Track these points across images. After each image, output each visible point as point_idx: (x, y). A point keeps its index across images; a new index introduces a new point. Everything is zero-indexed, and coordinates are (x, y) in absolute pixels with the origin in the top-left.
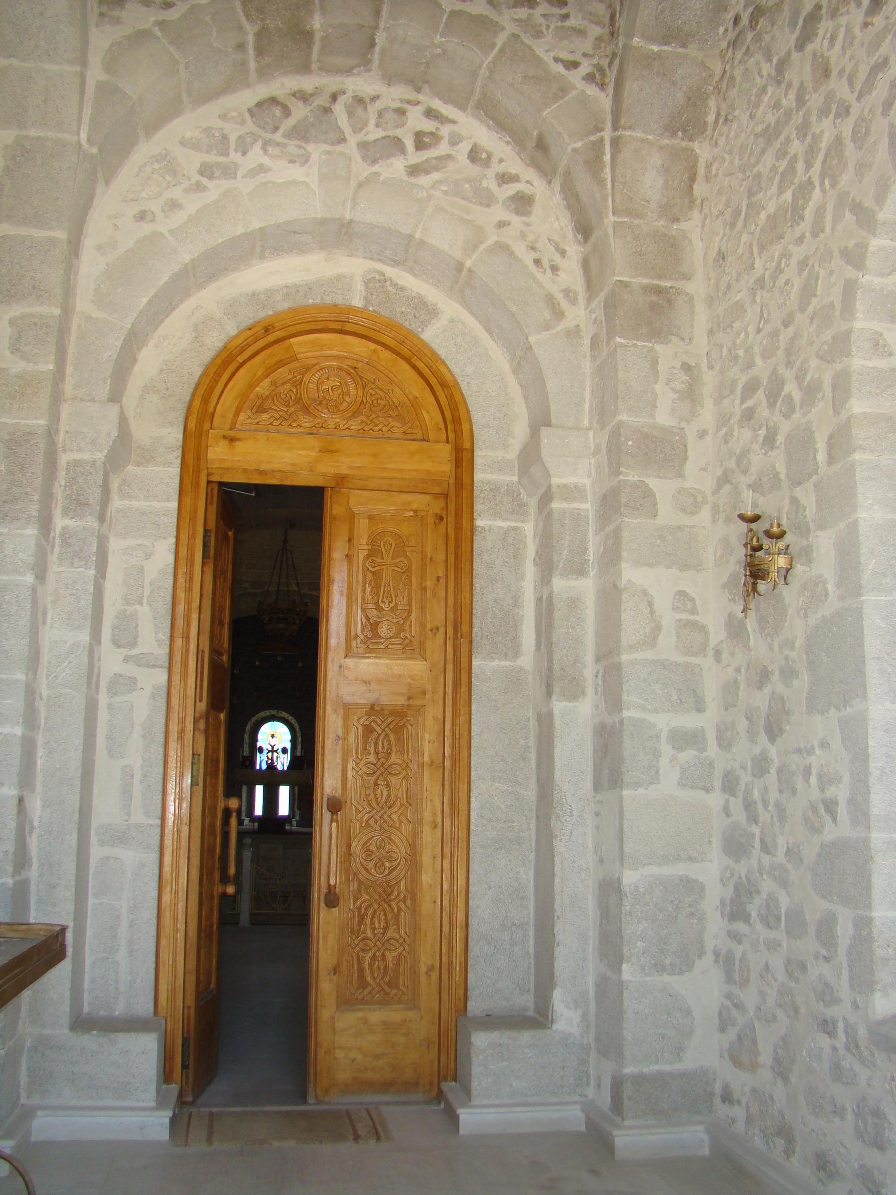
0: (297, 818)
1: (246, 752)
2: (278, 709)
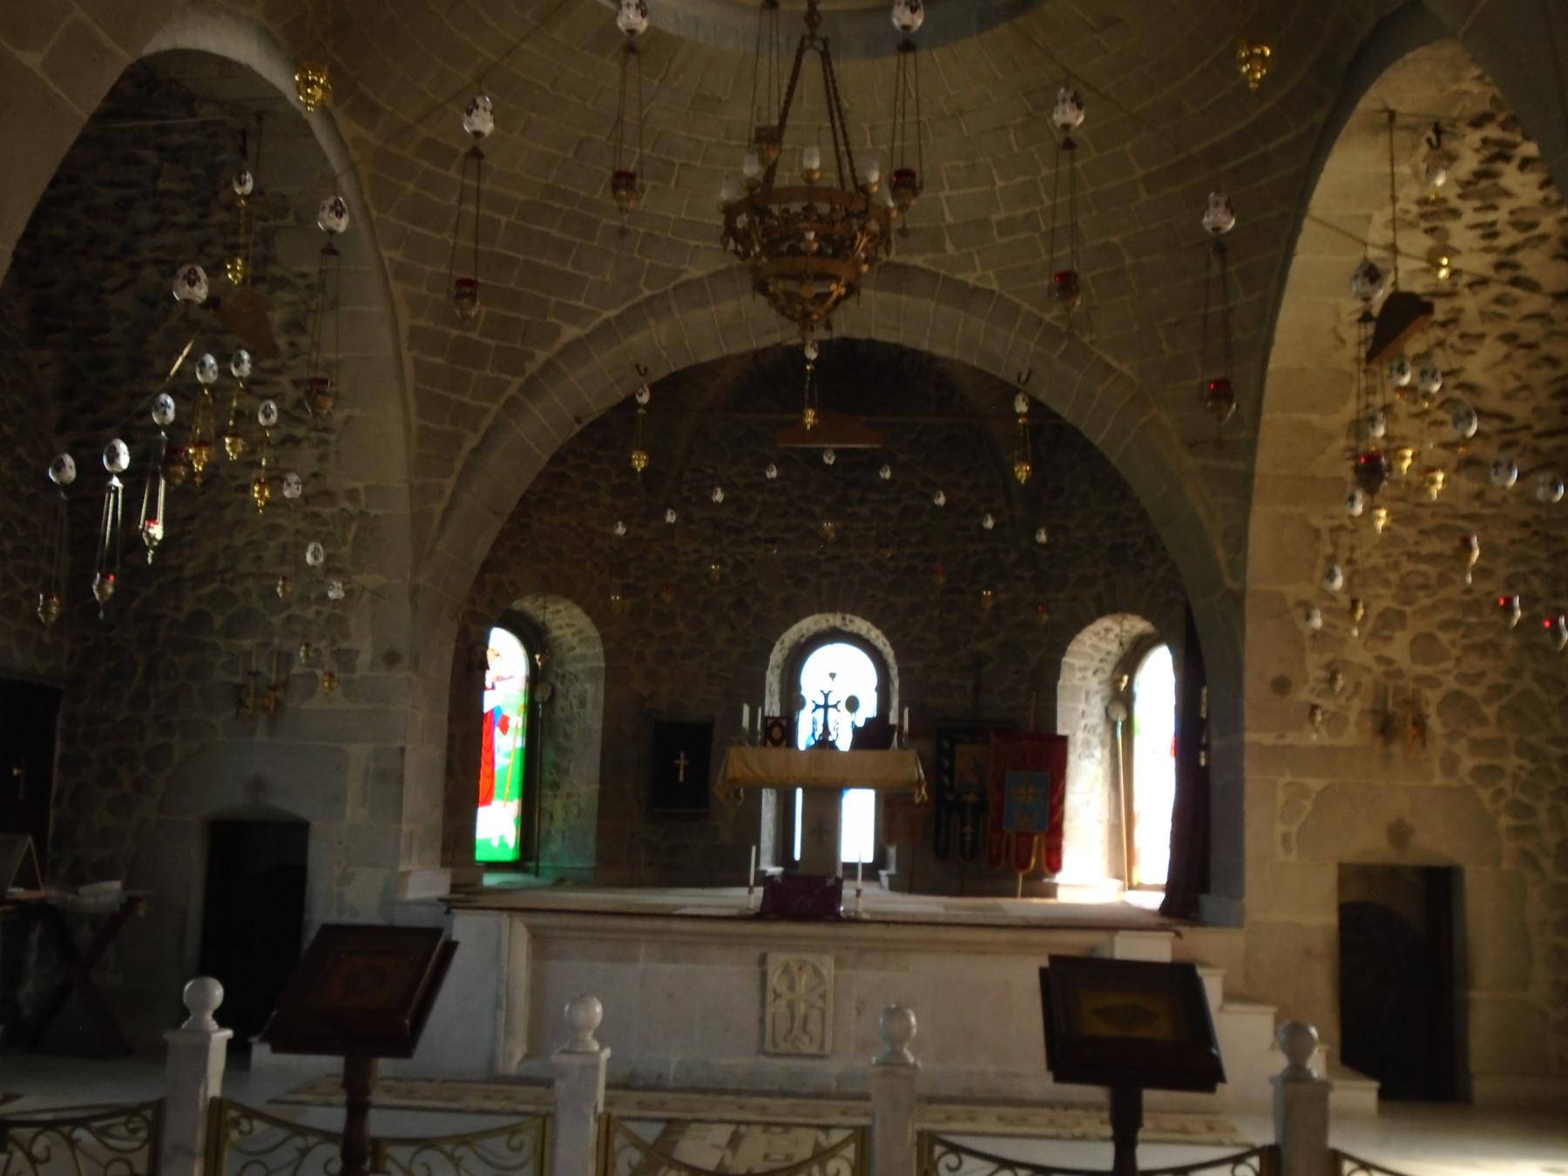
0: (892, 870)
1: (772, 707)
2: (844, 610)
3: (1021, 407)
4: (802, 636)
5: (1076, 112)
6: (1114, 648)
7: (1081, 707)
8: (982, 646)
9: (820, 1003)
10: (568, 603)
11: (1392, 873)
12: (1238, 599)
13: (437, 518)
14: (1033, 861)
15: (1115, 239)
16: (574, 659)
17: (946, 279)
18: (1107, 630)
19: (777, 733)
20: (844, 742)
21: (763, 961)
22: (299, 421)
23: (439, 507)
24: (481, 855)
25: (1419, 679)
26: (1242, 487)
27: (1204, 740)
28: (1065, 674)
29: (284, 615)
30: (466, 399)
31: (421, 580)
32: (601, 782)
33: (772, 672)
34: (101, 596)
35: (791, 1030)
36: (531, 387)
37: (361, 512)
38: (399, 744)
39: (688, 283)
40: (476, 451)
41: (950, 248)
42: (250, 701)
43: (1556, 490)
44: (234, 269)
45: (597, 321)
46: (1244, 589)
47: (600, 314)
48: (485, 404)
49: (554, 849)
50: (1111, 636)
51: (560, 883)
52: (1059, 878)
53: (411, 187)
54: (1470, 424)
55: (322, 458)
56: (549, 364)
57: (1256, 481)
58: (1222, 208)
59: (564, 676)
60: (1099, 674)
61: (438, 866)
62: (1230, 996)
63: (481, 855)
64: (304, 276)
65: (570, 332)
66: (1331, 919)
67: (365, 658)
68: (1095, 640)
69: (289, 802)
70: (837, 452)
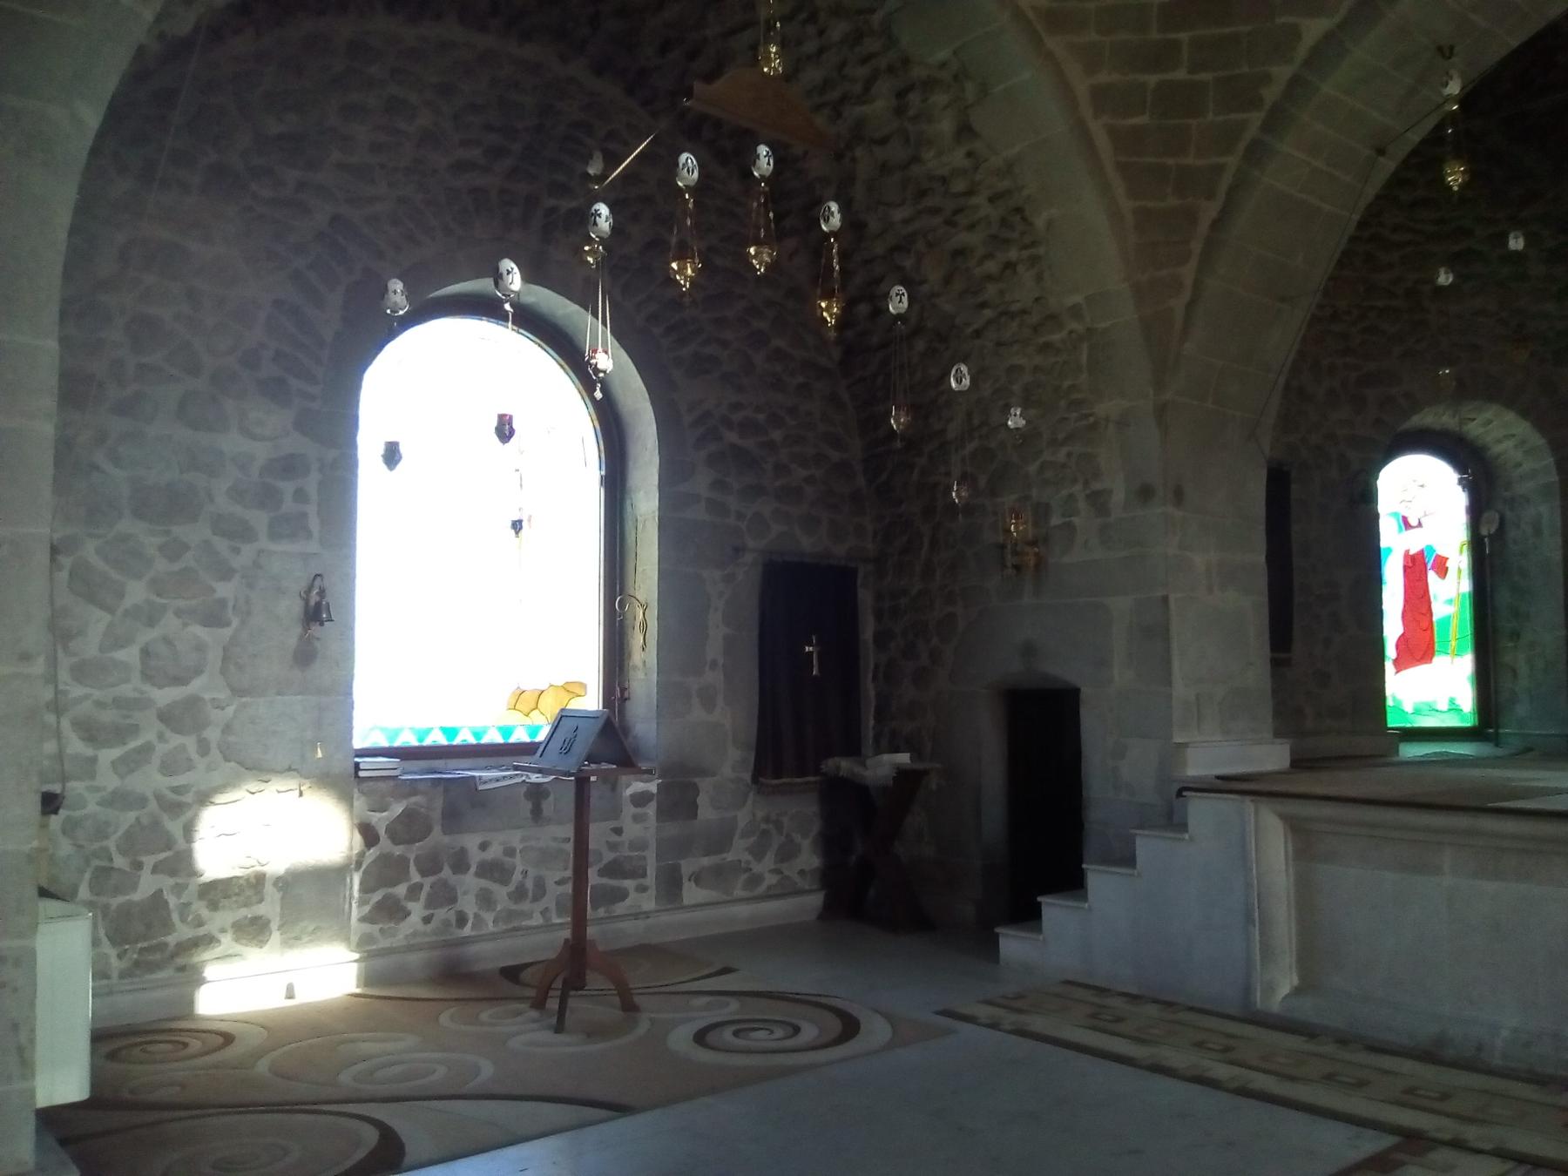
22: (1007, 241)
23: (1178, 304)
24: (1393, 721)
29: (1038, 463)
30: (1190, 160)
36: (1277, 121)
37: (1088, 329)
40: (1217, 224)
44: (768, 61)
48: (1221, 160)
49: (1521, 715)
55: (1039, 278)
56: (1295, 82)
63: (1393, 721)
64: (943, 65)
67: (1119, 496)
69: (1061, 668)
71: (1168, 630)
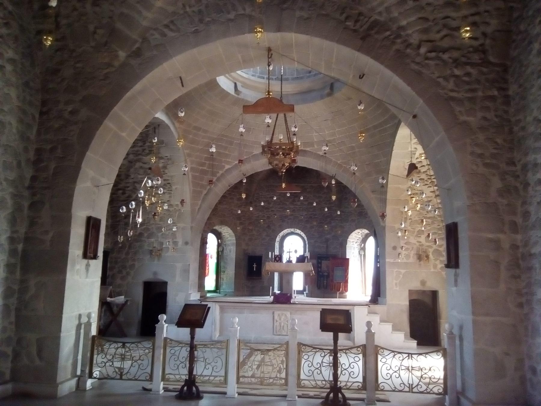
1: (277, 252)
3: (333, 182)
4: (284, 234)
5: (326, 148)
6: (360, 236)
7: (353, 251)
8: (328, 236)
9: (287, 323)
10: (227, 227)
11: (424, 292)
12: (384, 228)
13: (197, 210)
14: (341, 289)
15: (354, 145)
16: (228, 240)
17: (315, 153)
18: (359, 232)
19: (277, 259)
20: (294, 261)
21: (273, 313)
23: (197, 208)
25: (428, 246)
26: (384, 201)
27: (378, 261)
28: (348, 242)
31: (193, 225)
32: (235, 270)
33: (277, 243)
34: (130, 235)
35: (280, 329)
38: (189, 263)
39: (255, 155)
40: (206, 195)
41: (316, 146)
42: (153, 254)
43: (436, 212)
45: (234, 164)
46: (385, 226)
47: (234, 162)
49: (224, 287)
50: (360, 234)
51: (225, 295)
52: (347, 294)
53: (191, 136)
54: (423, 195)
55: (170, 197)
56: (222, 174)
57: (387, 200)
58: (354, 166)
59: (226, 245)
60: (357, 243)
61: (197, 291)
62: (382, 321)
65: (227, 167)
66: (408, 303)
68: (355, 235)
70: (291, 193)
71: (189, 271)
